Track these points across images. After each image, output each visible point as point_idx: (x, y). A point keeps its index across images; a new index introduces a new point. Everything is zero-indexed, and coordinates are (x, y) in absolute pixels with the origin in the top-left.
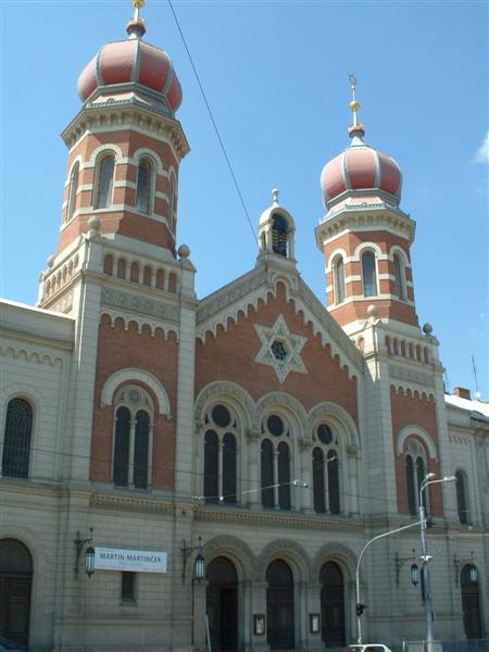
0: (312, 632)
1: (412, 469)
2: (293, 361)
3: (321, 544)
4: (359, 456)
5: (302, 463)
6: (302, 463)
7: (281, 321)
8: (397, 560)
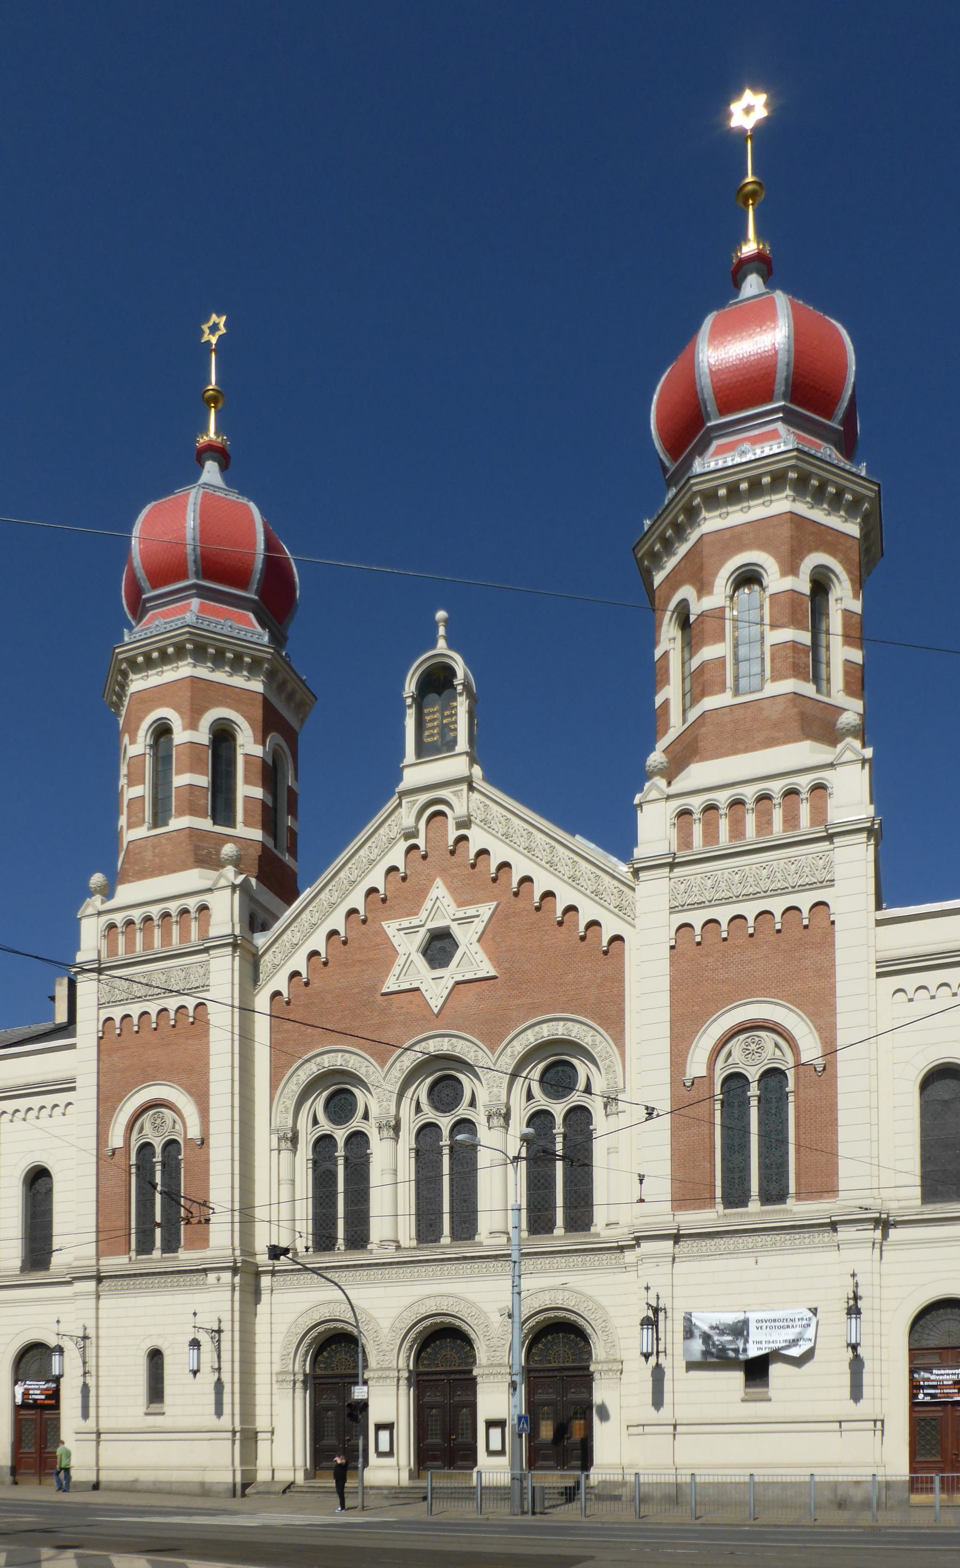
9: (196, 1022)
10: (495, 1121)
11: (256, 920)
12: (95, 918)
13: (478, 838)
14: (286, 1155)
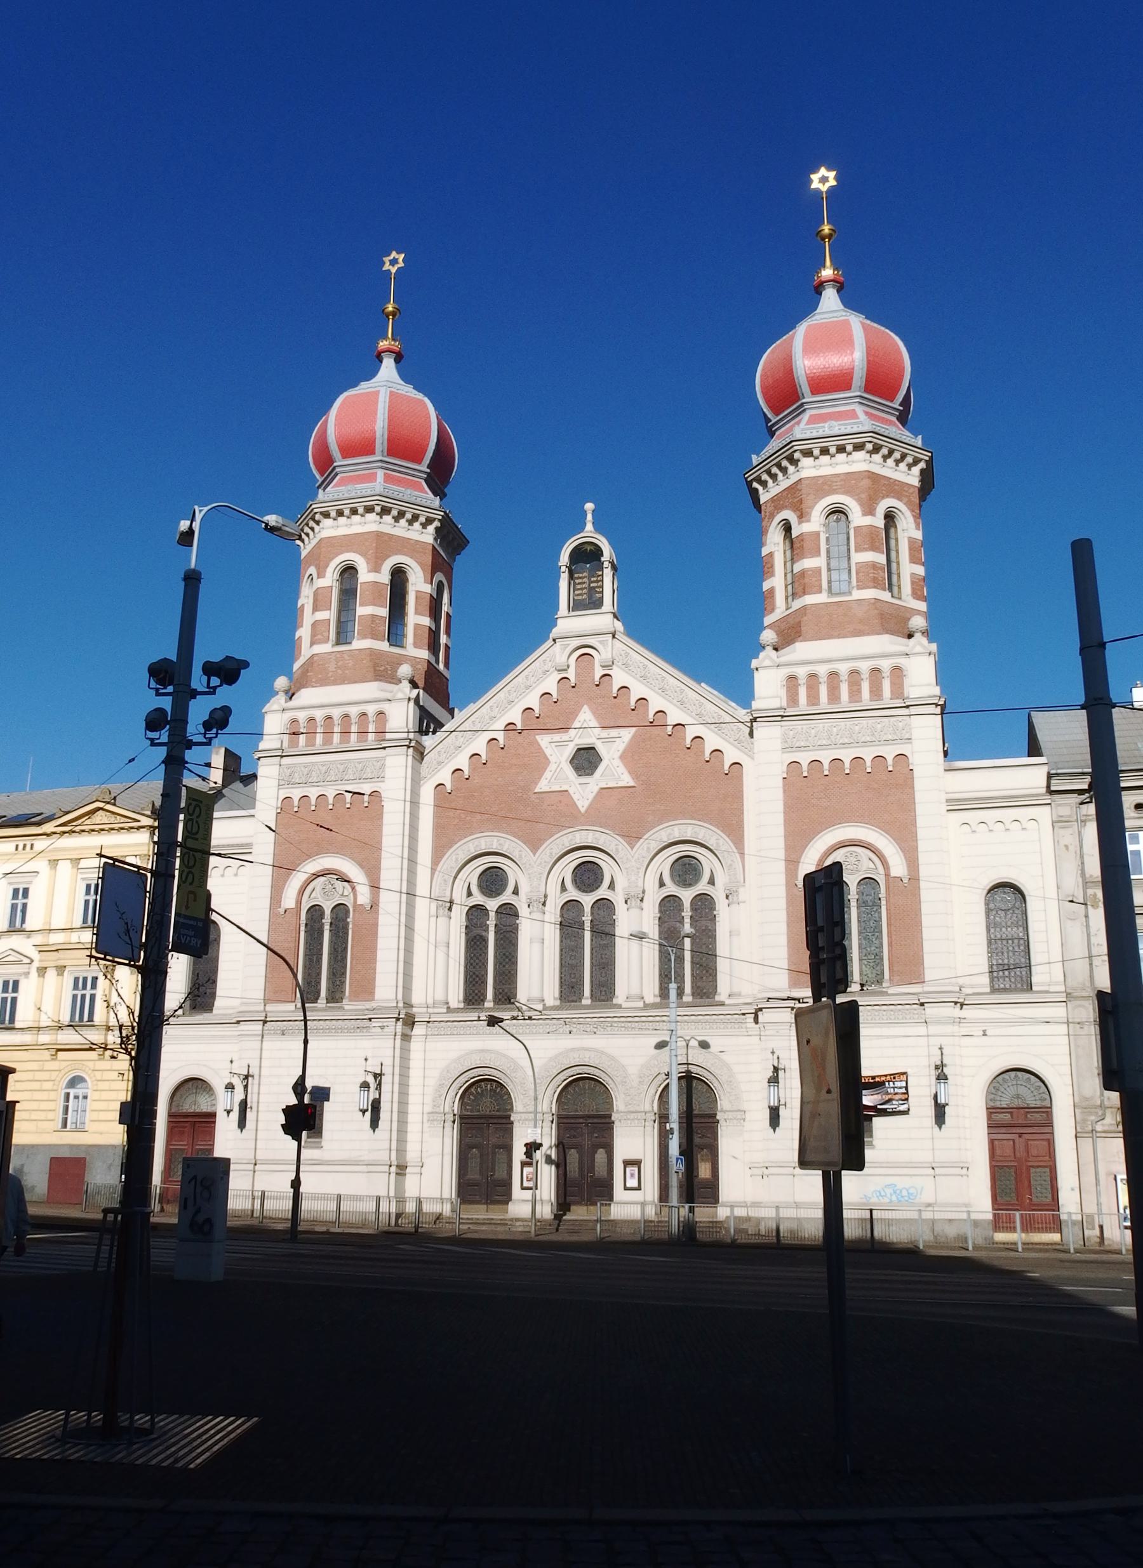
7: (586, 716)
9: (370, 806)
10: (633, 902)
11: (428, 723)
12: (279, 715)
13: (620, 678)
14: (442, 921)
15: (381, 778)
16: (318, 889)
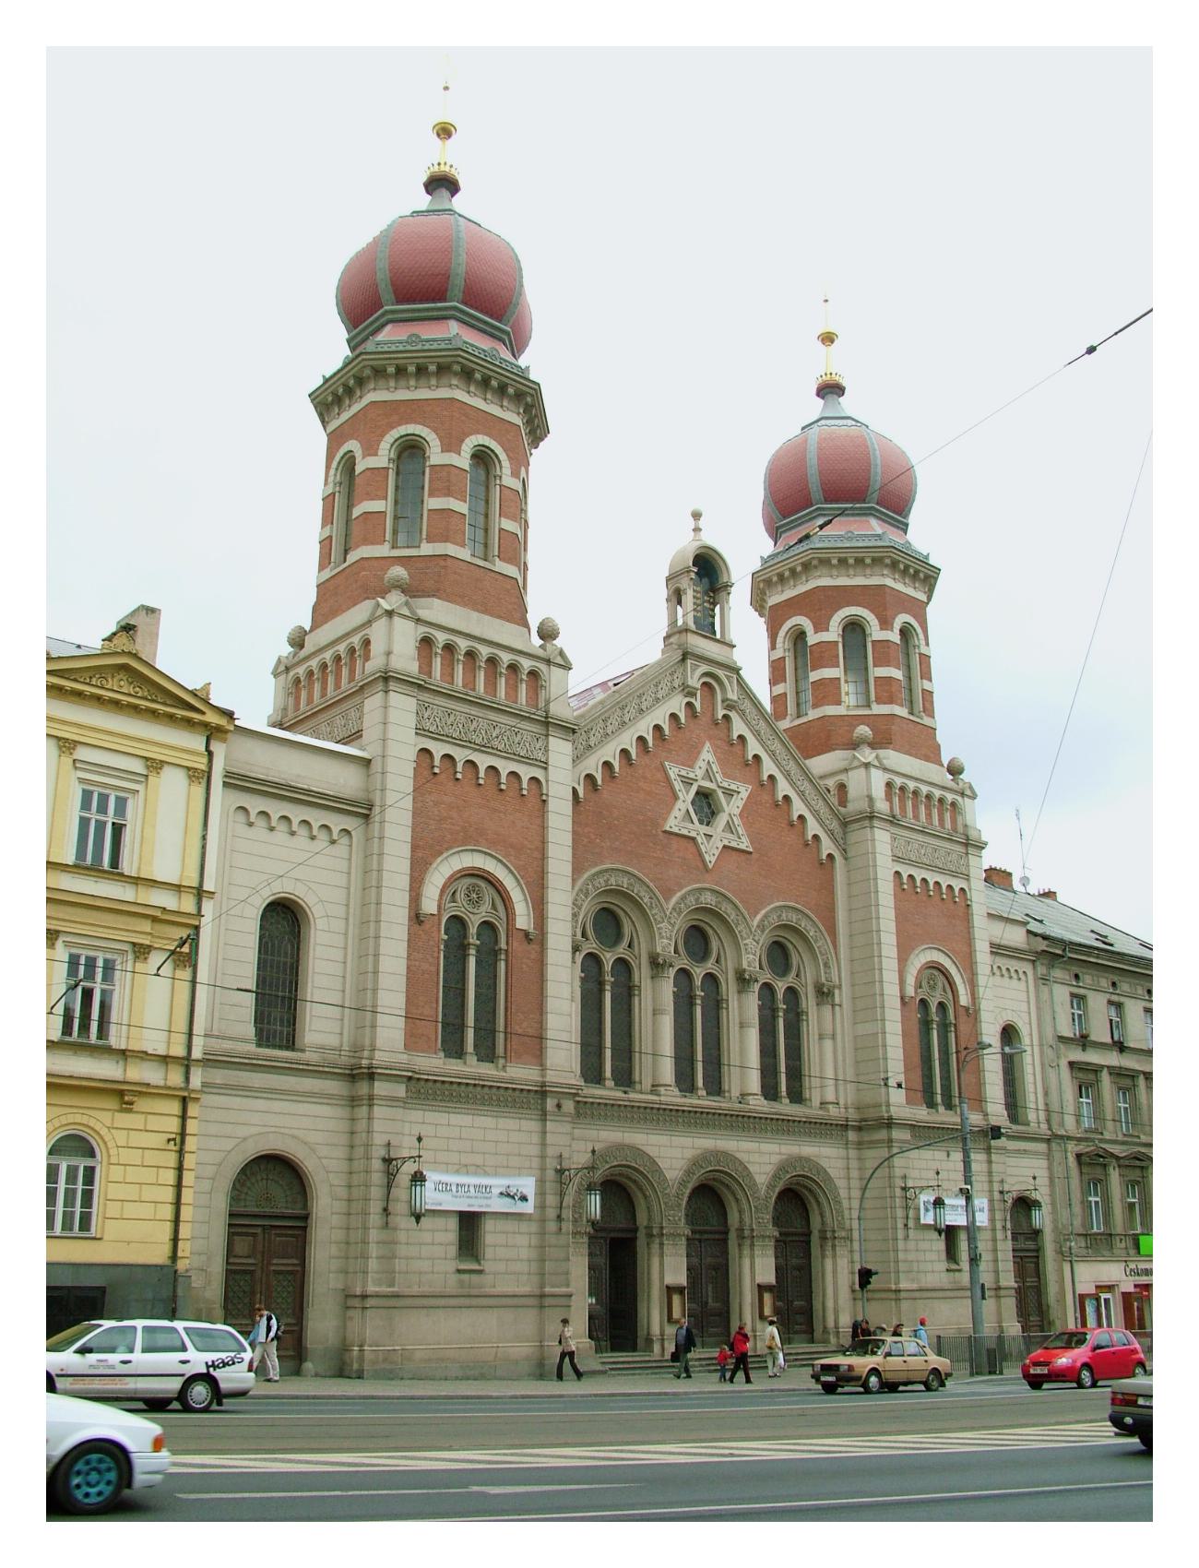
0: (762, 1317)
1: (939, 1026)
2: (729, 827)
3: (775, 1159)
4: (837, 1000)
5: (743, 1013)
6: (743, 1013)
7: (707, 754)
8: (904, 1189)
13: (739, 727)
15: (545, 766)
16: (460, 896)
